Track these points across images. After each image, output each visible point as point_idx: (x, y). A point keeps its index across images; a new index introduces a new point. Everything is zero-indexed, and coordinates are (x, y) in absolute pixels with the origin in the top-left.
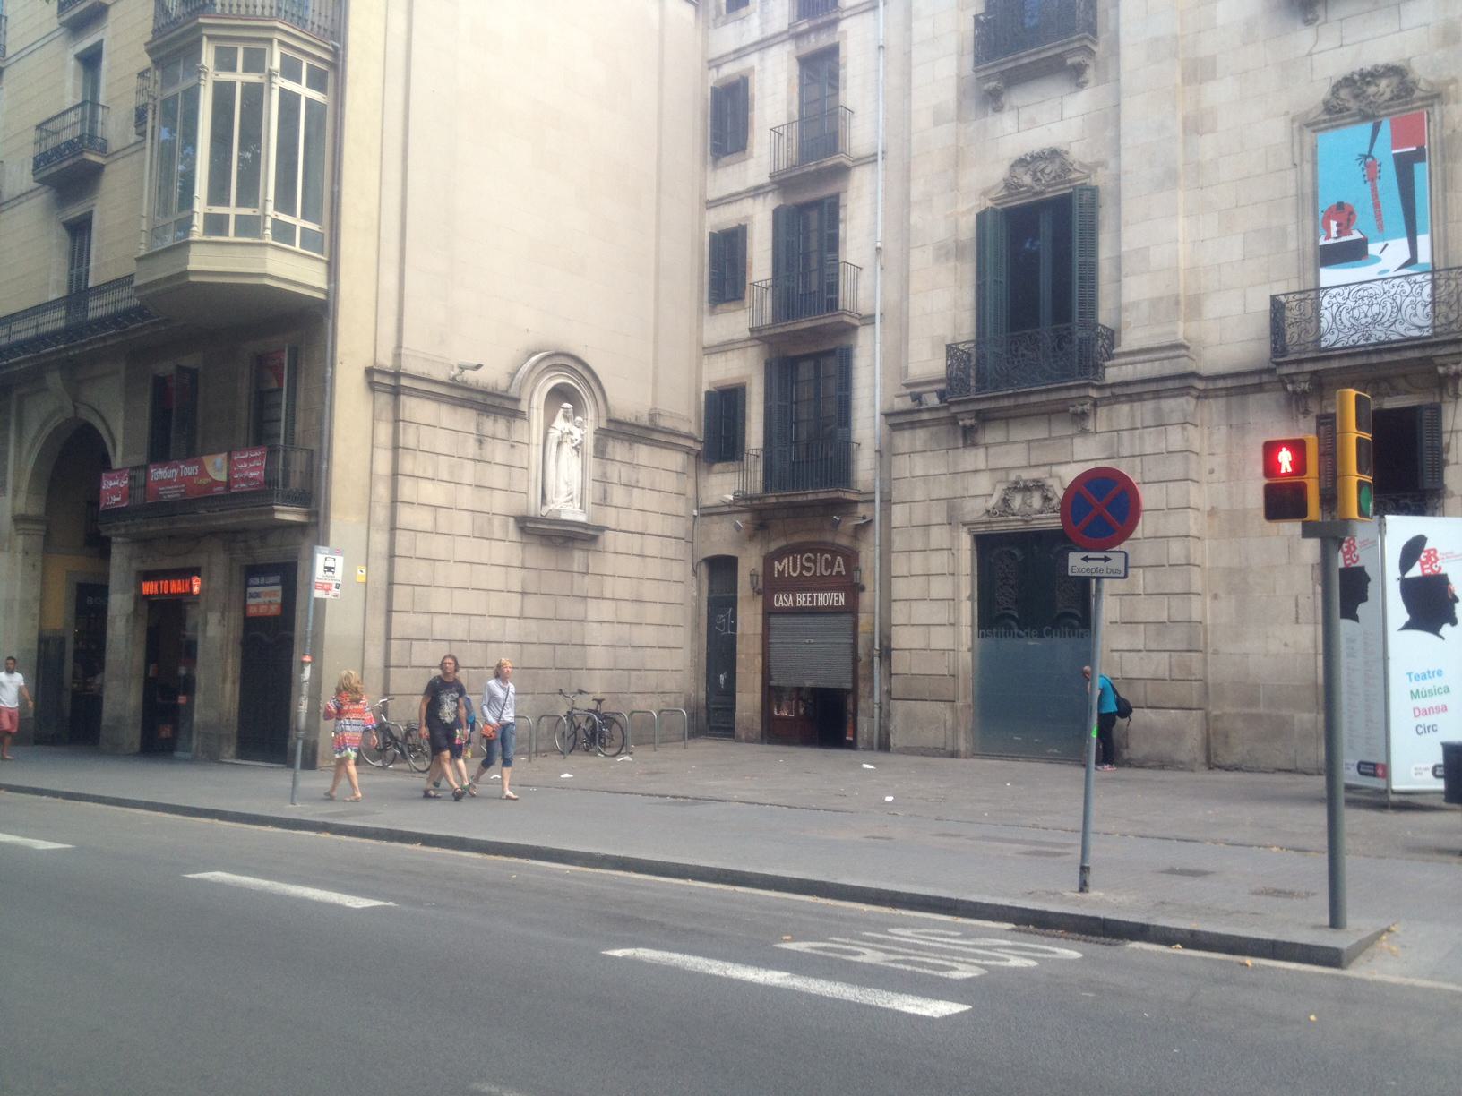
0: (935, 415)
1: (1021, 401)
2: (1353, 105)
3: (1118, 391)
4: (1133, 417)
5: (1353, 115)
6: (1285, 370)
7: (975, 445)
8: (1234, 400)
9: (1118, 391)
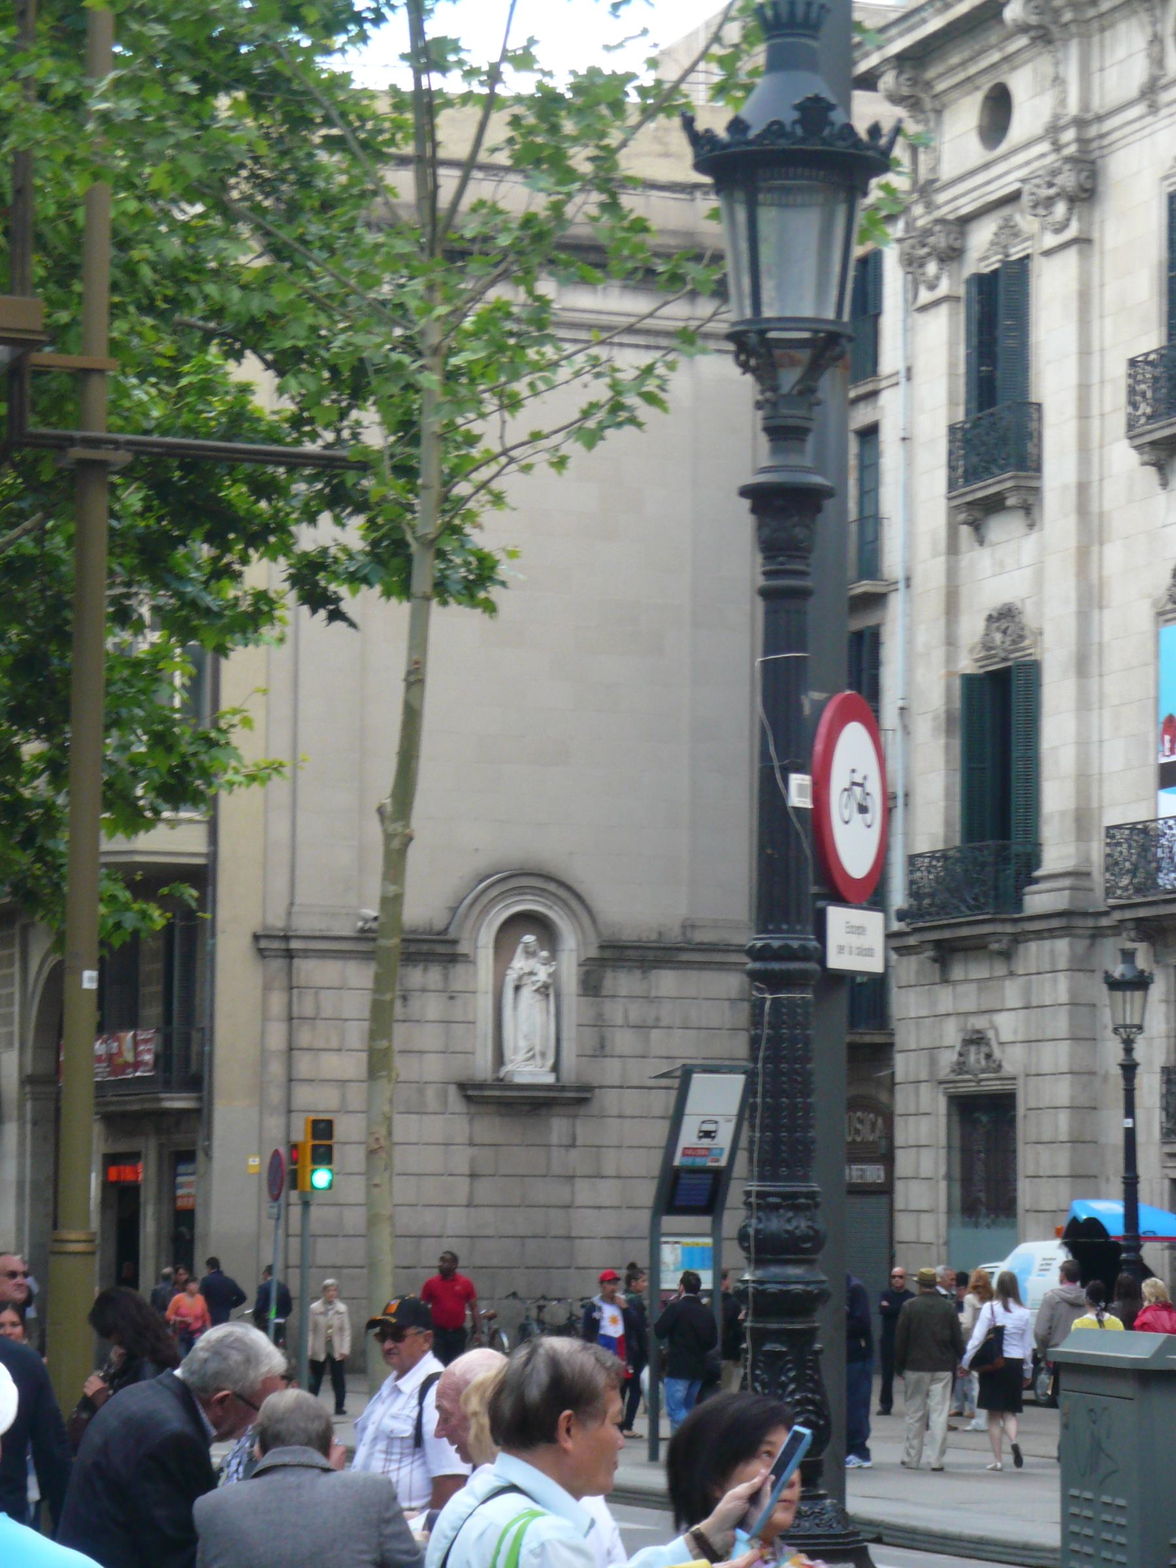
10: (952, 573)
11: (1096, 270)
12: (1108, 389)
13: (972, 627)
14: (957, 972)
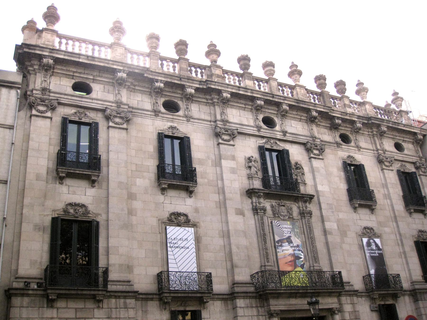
0: (35, 292)
1: (79, 292)
2: (174, 220)
3: (112, 294)
4: (116, 305)
5: (175, 224)
6: (166, 295)
7: (52, 307)
8: (143, 302)
9: (112, 294)
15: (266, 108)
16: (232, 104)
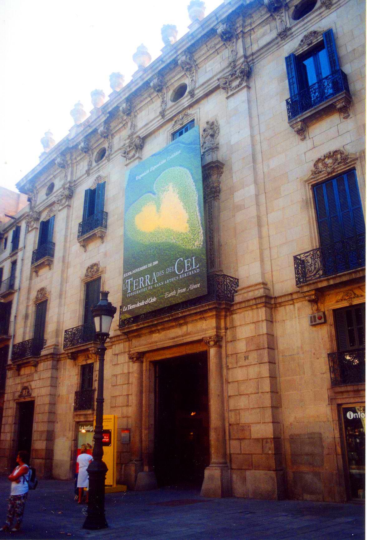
10: (30, 284)
11: (71, 213)
12: (72, 235)
13: (34, 294)
14: (22, 372)
15: (170, 80)
16: (139, 107)
